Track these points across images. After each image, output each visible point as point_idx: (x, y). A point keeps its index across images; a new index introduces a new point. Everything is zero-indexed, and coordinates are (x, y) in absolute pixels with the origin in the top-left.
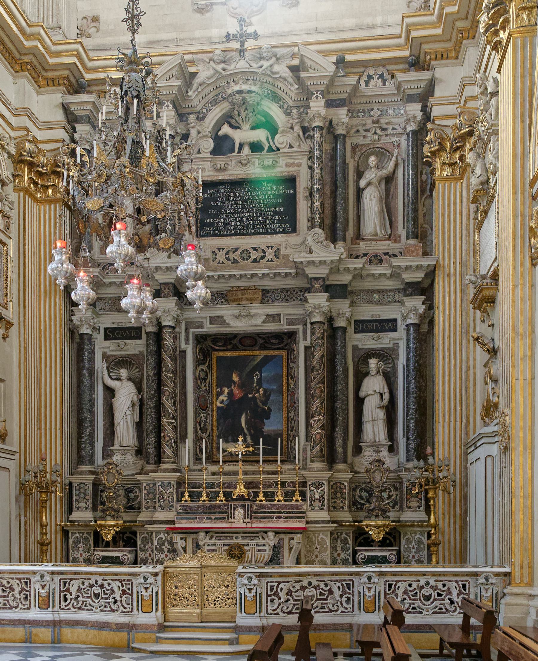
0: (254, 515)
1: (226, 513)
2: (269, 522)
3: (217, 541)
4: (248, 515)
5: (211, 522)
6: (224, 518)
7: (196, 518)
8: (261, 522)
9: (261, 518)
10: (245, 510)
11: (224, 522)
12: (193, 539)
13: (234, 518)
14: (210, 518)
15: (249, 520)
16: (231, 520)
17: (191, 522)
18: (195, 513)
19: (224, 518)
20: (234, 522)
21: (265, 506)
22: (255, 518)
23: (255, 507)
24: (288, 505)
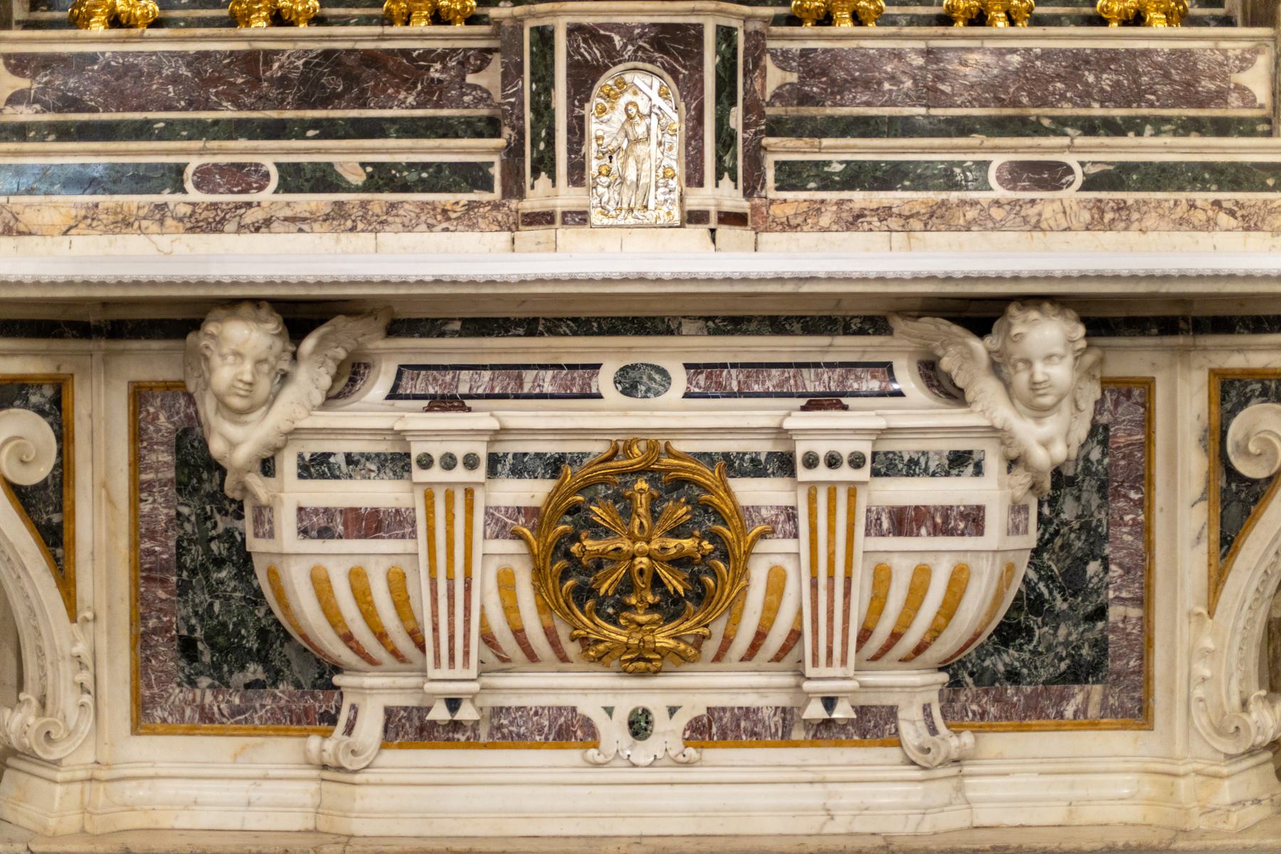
0: (781, 150)
1: (491, 127)
2: (936, 218)
3: (414, 418)
4: (725, 140)
5: (338, 215)
6: (474, 177)
7: (174, 177)
8: (854, 221)
9: (857, 176)
10: (690, 89)
11: (469, 218)
12: (139, 395)
13: (577, 173)
14: (324, 179)
15: (729, 196)
16: (539, 195)
17: (124, 223)
18: (171, 131)
19: (474, 177)
20: (580, 218)
21: (871, 61)
22: (791, 176)
23: (775, 77)
24: (1105, 60)
